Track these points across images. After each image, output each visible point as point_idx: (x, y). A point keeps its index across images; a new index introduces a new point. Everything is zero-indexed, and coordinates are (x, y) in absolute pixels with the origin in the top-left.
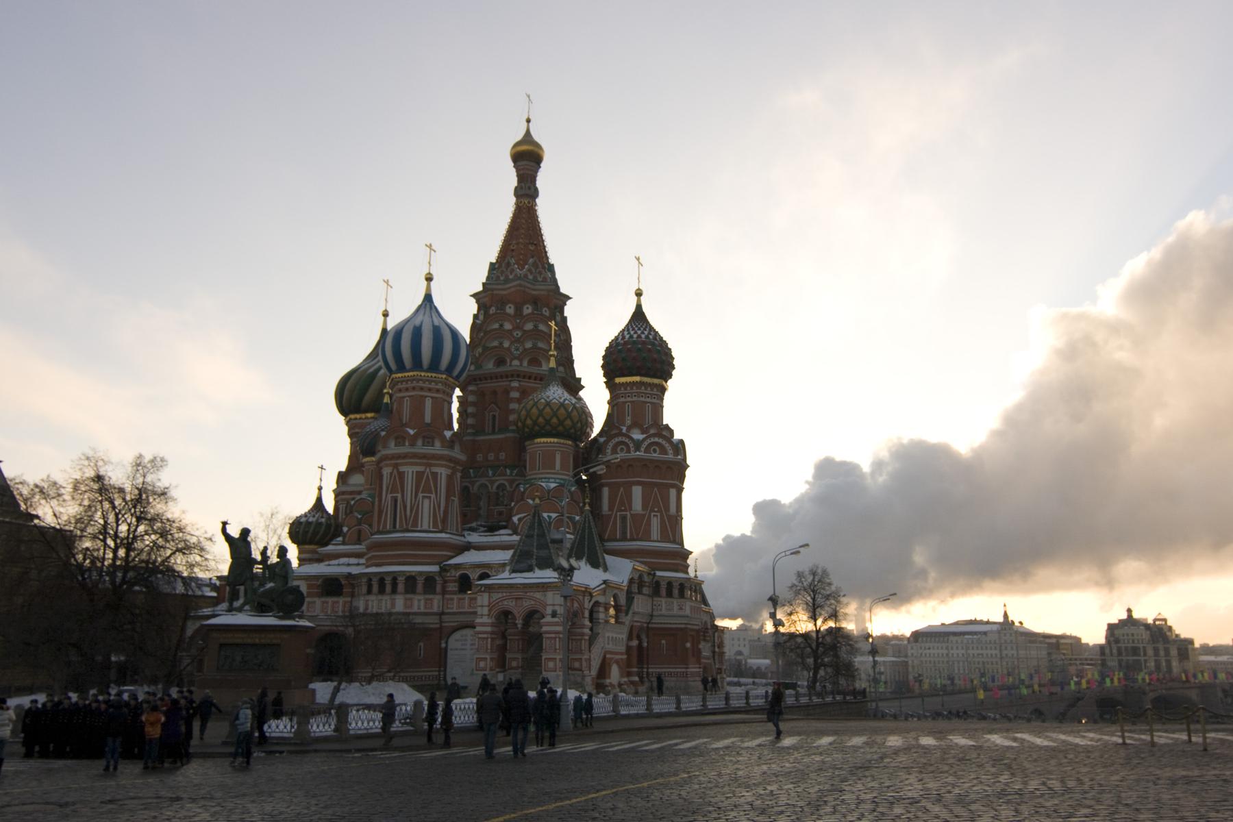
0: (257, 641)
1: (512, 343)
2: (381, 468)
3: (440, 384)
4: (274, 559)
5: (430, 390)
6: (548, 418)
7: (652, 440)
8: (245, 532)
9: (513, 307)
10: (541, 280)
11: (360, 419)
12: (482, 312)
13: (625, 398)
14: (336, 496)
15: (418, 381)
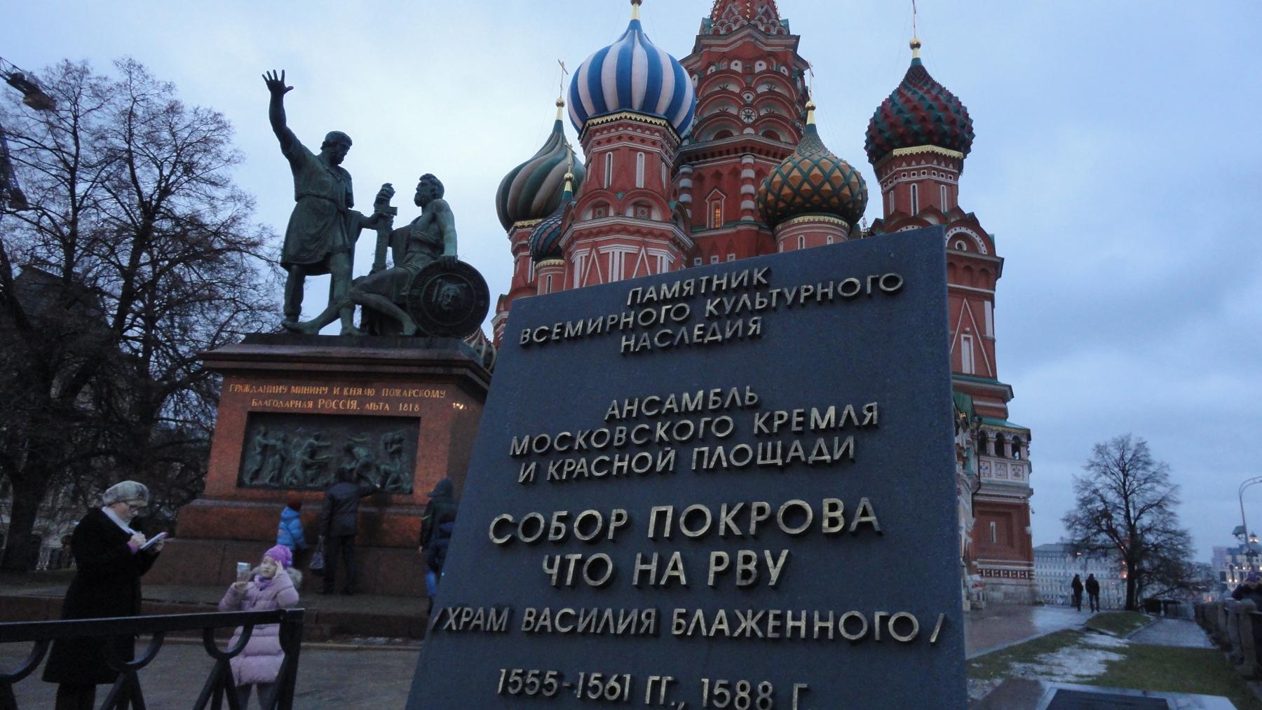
0: (353, 405)
1: (741, 108)
2: (570, 254)
3: (657, 134)
4: (406, 213)
5: (643, 141)
6: (817, 184)
7: (958, 230)
8: (338, 145)
9: (739, 63)
10: (775, 33)
11: (529, 226)
12: (696, 76)
13: (909, 176)
14: (495, 328)
15: (627, 126)
